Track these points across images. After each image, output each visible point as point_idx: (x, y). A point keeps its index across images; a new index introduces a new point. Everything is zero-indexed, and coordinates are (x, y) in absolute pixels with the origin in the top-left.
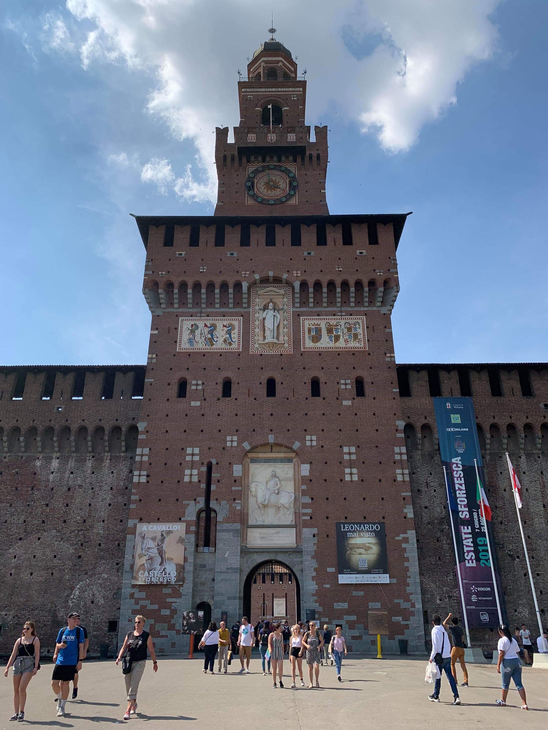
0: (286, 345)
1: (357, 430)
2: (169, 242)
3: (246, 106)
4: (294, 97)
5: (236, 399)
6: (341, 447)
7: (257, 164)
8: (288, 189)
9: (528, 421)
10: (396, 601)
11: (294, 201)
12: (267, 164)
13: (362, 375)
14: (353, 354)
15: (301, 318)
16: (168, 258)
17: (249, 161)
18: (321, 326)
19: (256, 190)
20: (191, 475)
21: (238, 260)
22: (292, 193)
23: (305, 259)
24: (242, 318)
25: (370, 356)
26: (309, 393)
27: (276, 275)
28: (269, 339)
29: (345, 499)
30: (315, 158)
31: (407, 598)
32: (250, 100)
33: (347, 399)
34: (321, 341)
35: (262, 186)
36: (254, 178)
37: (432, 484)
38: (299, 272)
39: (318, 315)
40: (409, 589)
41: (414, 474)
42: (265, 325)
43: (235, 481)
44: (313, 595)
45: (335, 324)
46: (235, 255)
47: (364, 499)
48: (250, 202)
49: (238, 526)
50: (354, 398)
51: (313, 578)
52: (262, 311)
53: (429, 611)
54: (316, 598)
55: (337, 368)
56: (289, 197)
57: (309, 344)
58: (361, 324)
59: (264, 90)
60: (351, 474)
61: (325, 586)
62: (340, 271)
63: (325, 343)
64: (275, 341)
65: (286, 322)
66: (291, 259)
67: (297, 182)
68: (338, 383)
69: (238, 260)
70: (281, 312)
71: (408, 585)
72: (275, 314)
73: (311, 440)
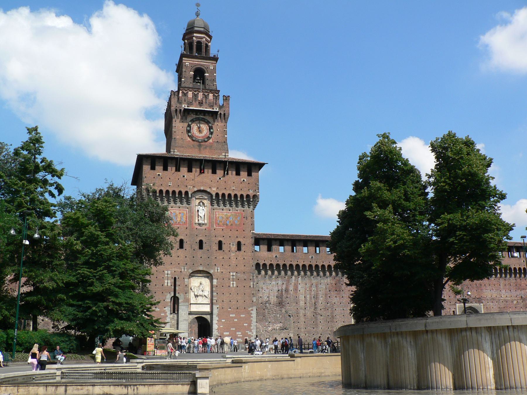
1: (237, 266)
2: (153, 168)
4: (211, 67)
5: (186, 250)
6: (230, 272)
9: (304, 263)
10: (247, 332)
11: (211, 141)
16: (154, 176)
17: (188, 114)
20: (168, 283)
22: (210, 136)
25: (244, 232)
26: (217, 248)
28: (201, 222)
30: (222, 116)
31: (251, 331)
32: (187, 66)
36: (191, 125)
37: (264, 288)
38: (215, 188)
40: (252, 328)
41: (257, 283)
42: (199, 214)
43: (186, 286)
44: (216, 330)
46: (185, 176)
48: (189, 139)
49: (187, 304)
51: (216, 324)
53: (258, 335)
54: (217, 331)
56: (209, 138)
61: (221, 326)
64: (203, 222)
70: (206, 207)
71: (252, 326)
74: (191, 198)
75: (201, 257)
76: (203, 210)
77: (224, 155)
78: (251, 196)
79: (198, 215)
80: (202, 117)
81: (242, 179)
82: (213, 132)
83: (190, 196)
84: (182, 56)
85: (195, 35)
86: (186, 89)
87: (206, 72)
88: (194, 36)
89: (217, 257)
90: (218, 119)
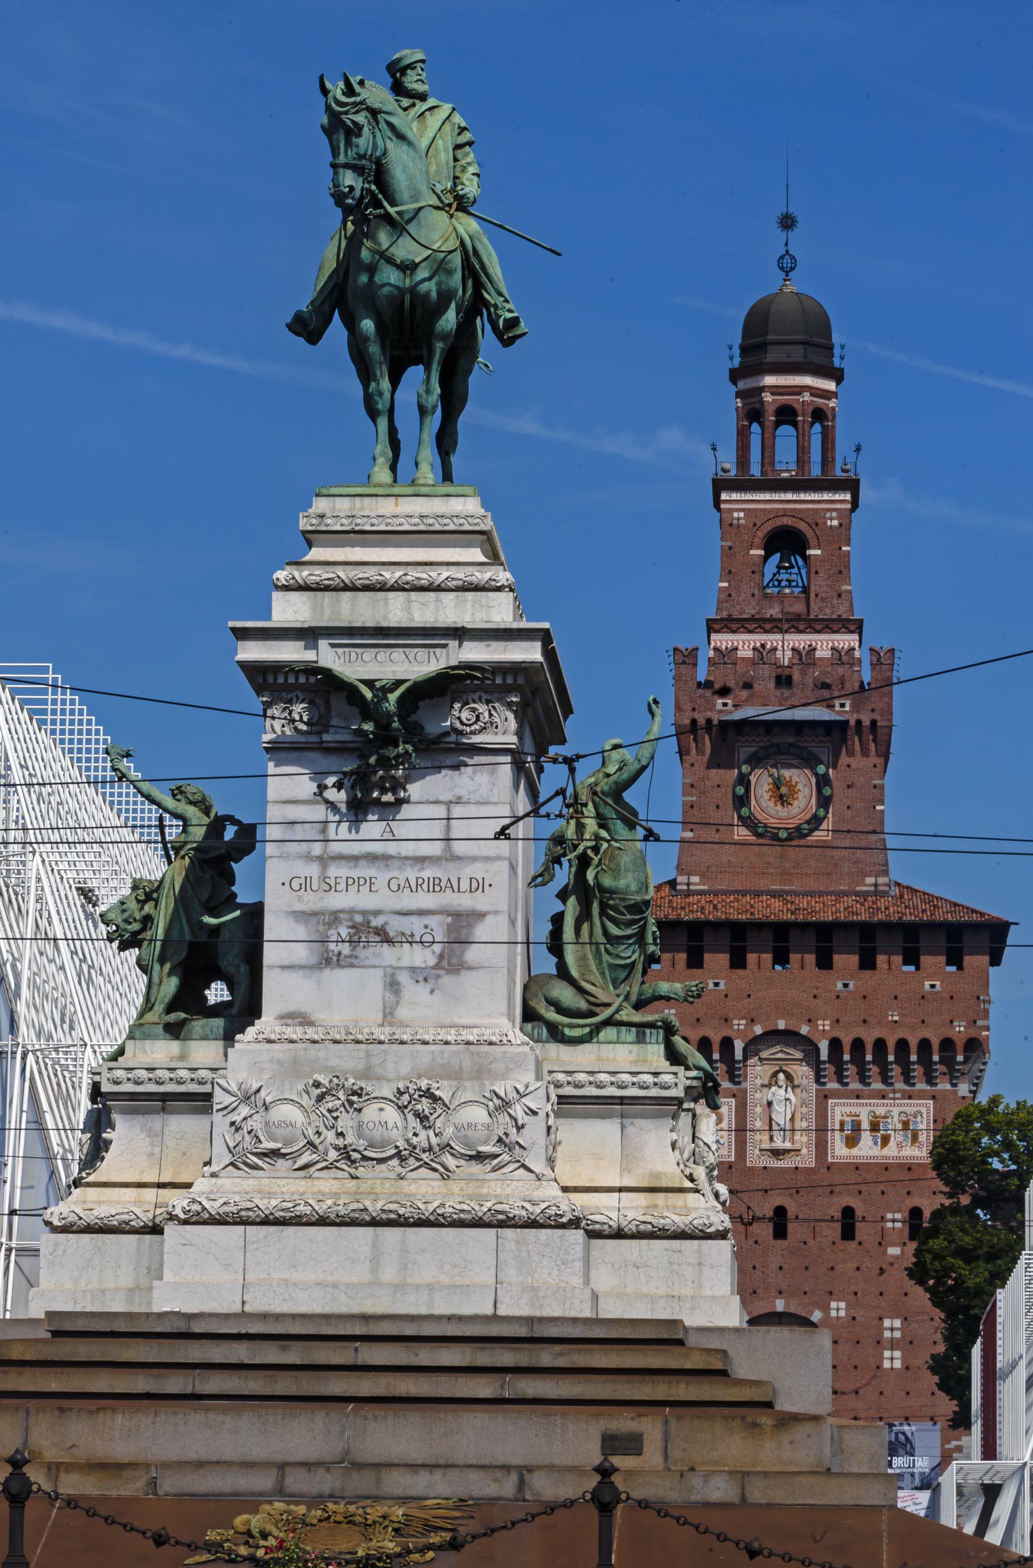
0: (804, 1151)
1: (906, 1294)
3: (729, 544)
4: (831, 519)
7: (754, 737)
8: (814, 801)
12: (775, 740)
13: (919, 1205)
14: (909, 1169)
15: (830, 1101)
18: (861, 1118)
19: (753, 802)
21: (726, 996)
22: (822, 812)
23: (838, 997)
24: (733, 1100)
27: (789, 1028)
29: (881, 1393)
30: (866, 731)
32: (738, 526)
33: (894, 1245)
34: (860, 1145)
35: (765, 794)
36: (750, 774)
38: (827, 1022)
39: (858, 1097)
42: (773, 1117)
45: (883, 1114)
46: (722, 986)
47: (908, 1393)
50: (904, 1244)
52: (765, 1090)
55: (883, 1193)
56: (816, 821)
57: (839, 1150)
58: (925, 1115)
59: (767, 496)
60: (892, 1359)
62: (896, 1022)
63: (867, 1149)
64: (788, 1145)
65: (804, 1110)
66: (815, 997)
67: (832, 788)
68: (882, 1218)
69: (726, 996)
70: (798, 1091)
72: (788, 1096)
73: (839, 1309)
74: (745, 1058)
75: (781, 1268)
76: (787, 1100)
77: (870, 885)
78: (960, 1044)
79: (771, 1119)
80: (791, 740)
81: (927, 984)
82: (832, 795)
83: (738, 1054)
84: (719, 485)
85: (770, 380)
86: (734, 626)
87: (813, 541)
88: (762, 389)
89: (837, 1267)
90: (850, 743)
